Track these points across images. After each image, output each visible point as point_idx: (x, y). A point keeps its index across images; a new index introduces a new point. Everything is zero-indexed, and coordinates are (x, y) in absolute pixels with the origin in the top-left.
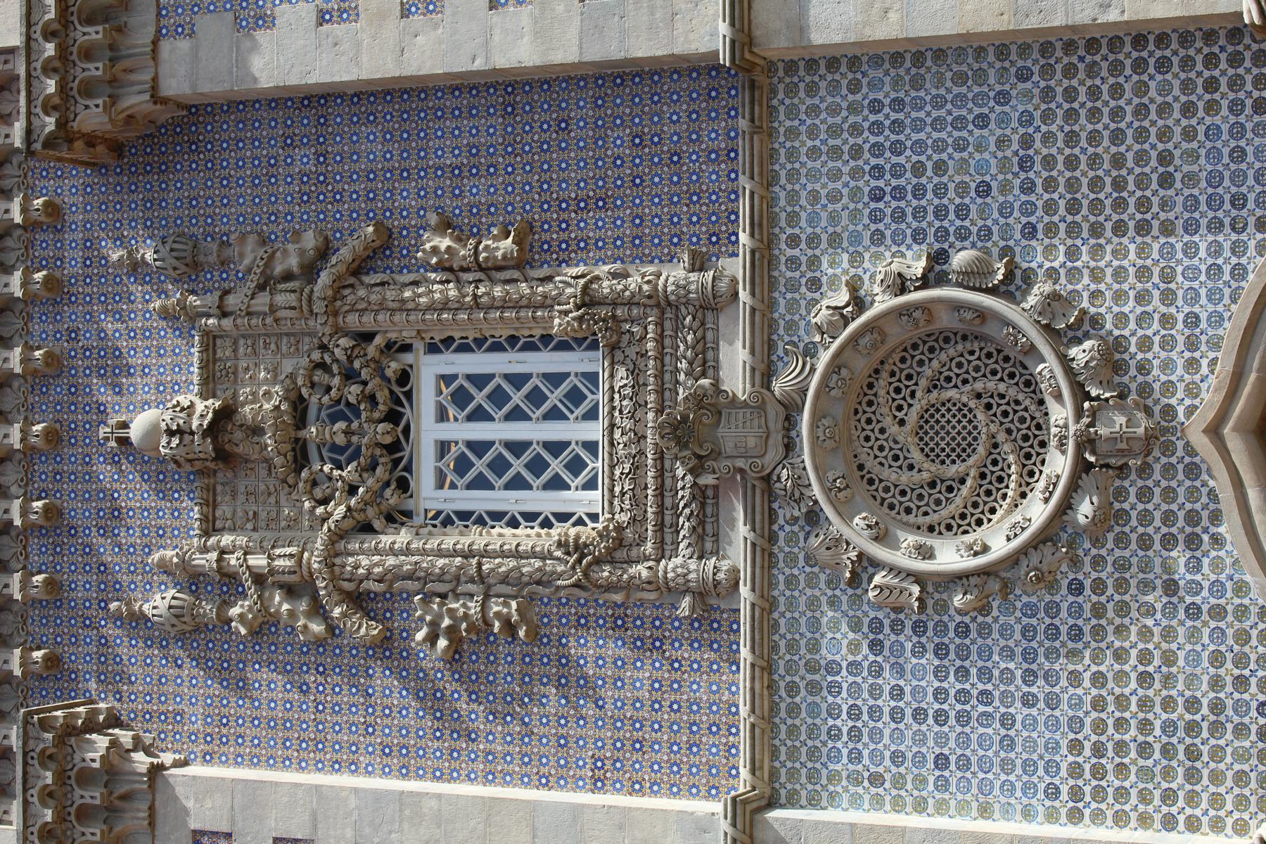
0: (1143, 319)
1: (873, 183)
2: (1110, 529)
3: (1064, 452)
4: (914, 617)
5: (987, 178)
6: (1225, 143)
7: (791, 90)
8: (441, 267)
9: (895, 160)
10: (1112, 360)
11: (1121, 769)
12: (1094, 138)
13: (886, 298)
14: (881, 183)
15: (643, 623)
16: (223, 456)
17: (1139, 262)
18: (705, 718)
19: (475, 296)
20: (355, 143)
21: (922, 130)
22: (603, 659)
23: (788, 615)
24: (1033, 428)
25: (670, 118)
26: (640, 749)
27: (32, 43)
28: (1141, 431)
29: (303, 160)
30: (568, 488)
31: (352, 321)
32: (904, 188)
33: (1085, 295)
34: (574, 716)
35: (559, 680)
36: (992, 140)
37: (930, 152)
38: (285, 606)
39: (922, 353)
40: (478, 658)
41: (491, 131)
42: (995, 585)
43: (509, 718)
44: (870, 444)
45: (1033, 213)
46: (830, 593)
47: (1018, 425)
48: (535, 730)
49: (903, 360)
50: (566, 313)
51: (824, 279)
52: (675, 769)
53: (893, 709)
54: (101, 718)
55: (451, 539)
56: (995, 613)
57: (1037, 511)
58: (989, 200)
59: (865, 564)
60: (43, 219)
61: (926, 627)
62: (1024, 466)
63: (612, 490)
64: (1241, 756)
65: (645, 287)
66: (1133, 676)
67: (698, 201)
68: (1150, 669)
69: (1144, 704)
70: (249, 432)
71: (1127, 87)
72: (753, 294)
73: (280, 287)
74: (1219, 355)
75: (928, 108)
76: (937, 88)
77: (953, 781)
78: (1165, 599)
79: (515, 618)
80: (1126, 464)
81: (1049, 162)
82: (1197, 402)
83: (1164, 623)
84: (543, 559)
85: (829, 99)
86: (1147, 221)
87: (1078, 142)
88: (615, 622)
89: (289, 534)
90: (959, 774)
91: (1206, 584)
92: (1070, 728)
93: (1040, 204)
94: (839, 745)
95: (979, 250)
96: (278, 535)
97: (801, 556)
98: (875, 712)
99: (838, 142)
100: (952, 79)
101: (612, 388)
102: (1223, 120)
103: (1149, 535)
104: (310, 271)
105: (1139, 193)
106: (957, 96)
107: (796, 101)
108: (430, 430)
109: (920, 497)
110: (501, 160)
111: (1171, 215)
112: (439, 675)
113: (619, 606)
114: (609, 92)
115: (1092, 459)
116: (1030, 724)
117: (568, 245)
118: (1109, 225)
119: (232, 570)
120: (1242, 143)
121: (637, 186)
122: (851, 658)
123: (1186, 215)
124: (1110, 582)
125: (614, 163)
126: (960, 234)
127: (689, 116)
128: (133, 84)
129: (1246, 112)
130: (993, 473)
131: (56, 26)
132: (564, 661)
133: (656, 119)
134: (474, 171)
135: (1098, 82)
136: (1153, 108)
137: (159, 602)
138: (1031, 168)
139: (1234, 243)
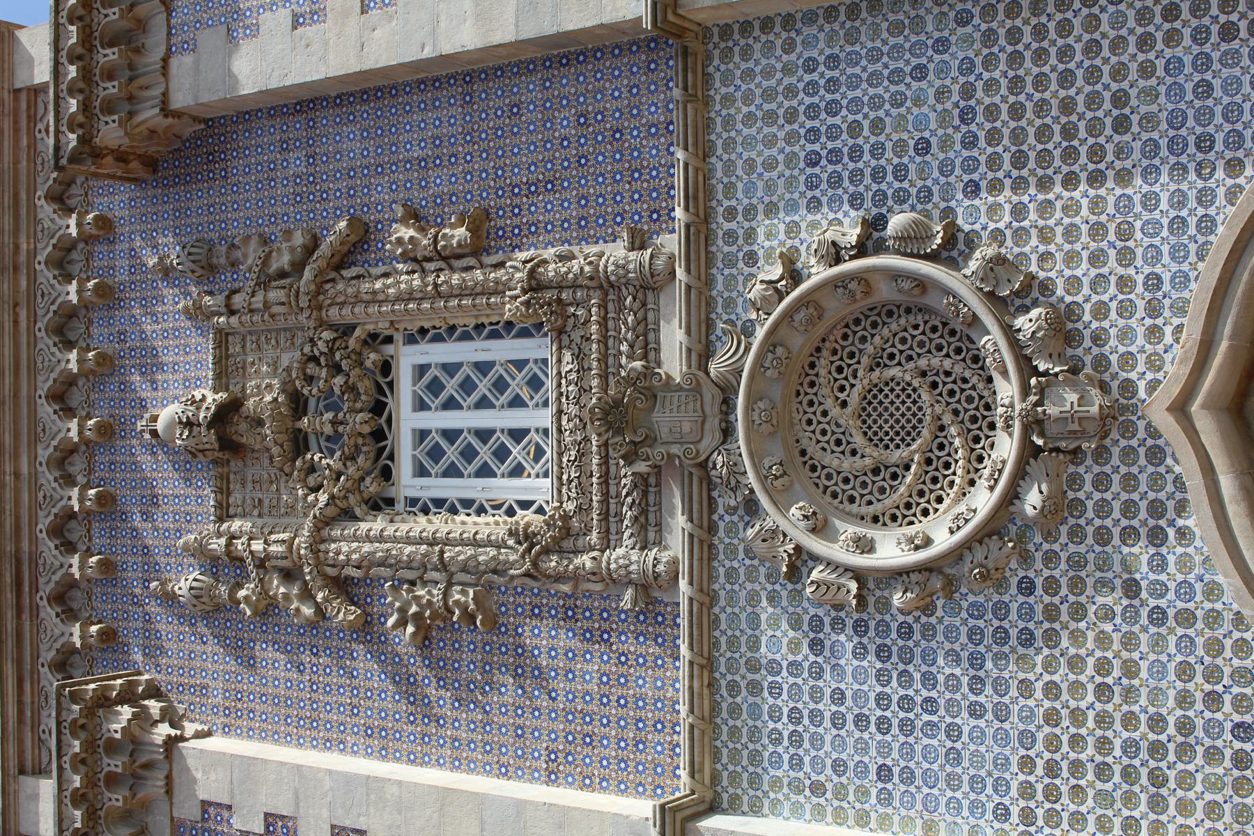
0: (1098, 283)
1: (809, 147)
2: (1064, 521)
3: (1010, 435)
4: (856, 616)
5: (927, 134)
6: (1189, 77)
7: (727, 55)
8: (405, 257)
9: (830, 121)
10: (1063, 329)
11: (1077, 791)
12: (1040, 82)
13: (821, 269)
14: (817, 147)
16: (230, 446)
18: (650, 715)
19: (436, 285)
20: (337, 142)
21: (857, 87)
22: (555, 650)
23: (729, 610)
24: (981, 409)
25: (612, 95)
26: (590, 744)
27: (61, 68)
28: (1095, 410)
29: (296, 163)
30: (495, 475)
32: (840, 150)
33: (1034, 257)
34: (530, 706)
35: (516, 670)
36: (931, 92)
37: (866, 109)
38: (282, 590)
39: (864, 329)
40: (445, 645)
41: (452, 121)
42: (937, 583)
43: (472, 706)
44: (812, 428)
45: (975, 170)
46: (769, 587)
47: (965, 405)
48: (496, 719)
49: (845, 337)
50: (516, 297)
51: (761, 253)
52: (623, 765)
53: (834, 714)
54: (140, 689)
55: (421, 525)
56: (940, 613)
57: (983, 500)
58: (928, 158)
60: (94, 232)
61: (867, 626)
62: (973, 450)
63: (560, 479)
64: (1214, 784)
65: (587, 269)
66: (1090, 687)
67: (639, 178)
68: (1109, 680)
69: (1103, 720)
70: (254, 424)
71: (1076, 22)
72: (688, 271)
73: (274, 284)
74: (1185, 321)
75: (864, 63)
76: (873, 40)
77: (897, 795)
78: (1125, 602)
80: (1080, 447)
81: (992, 112)
82: (1160, 376)
84: (499, 547)
85: (764, 62)
86: (1101, 171)
88: (566, 613)
89: (286, 520)
90: (903, 788)
91: (1172, 585)
92: (1021, 742)
93: (983, 159)
94: (780, 749)
95: (919, 213)
96: (278, 521)
97: (741, 548)
98: (815, 716)
99: (773, 106)
100: (888, 30)
101: (559, 373)
102: (1186, 50)
103: (1107, 528)
104: (298, 268)
105: (1091, 141)
106: (893, 47)
107: (731, 66)
108: (408, 420)
110: (460, 149)
112: (412, 661)
113: (569, 597)
114: (556, 72)
115: (1040, 442)
116: (978, 736)
117: (521, 230)
119: (239, 554)
120: (1208, 76)
121: (582, 166)
122: (791, 658)
124: (1064, 581)
125: (561, 144)
126: (899, 197)
127: (630, 91)
128: (148, 99)
129: (1212, 40)
130: (939, 458)
131: (80, 50)
132: (520, 650)
133: (599, 97)
134: (438, 162)
135: (1044, 19)
136: (1105, 43)
137: (184, 583)
138: (973, 120)
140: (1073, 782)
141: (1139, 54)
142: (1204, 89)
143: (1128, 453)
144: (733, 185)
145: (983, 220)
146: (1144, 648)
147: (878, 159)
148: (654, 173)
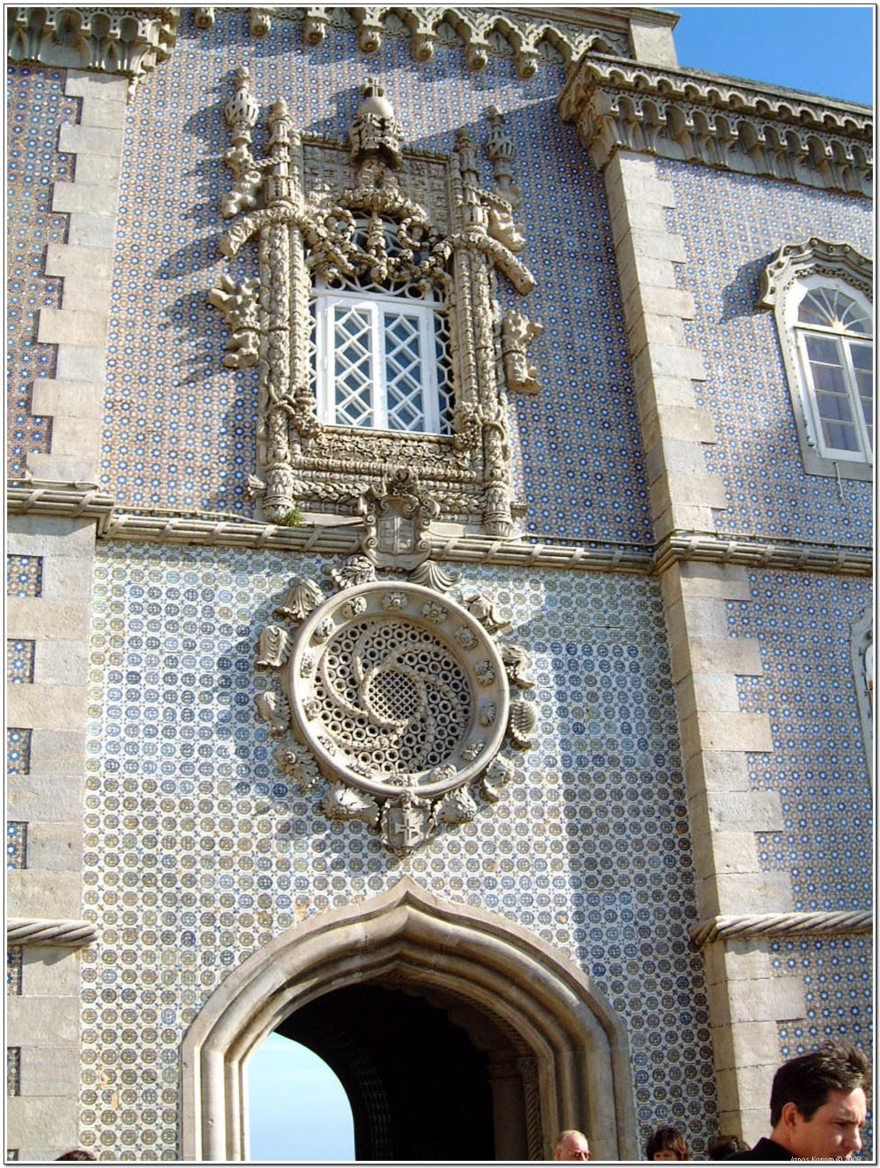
0: (490, 846)
1: (579, 647)
4: (251, 662)
5: (587, 732)
7: (641, 590)
9: (597, 664)
12: (618, 811)
16: (361, 158)
17: (532, 844)
29: (571, 243)
31: (462, 261)
49: (447, 664)
50: (476, 411)
56: (258, 726)
57: (340, 761)
58: (572, 732)
59: (295, 625)
64: (149, 918)
65: (499, 471)
68: (217, 848)
69: (188, 842)
79: (244, 350)
90: (124, 691)
91: (287, 893)
94: (145, 596)
101: (420, 441)
108: (373, 307)
115: (387, 805)
120: (619, 919)
122: (217, 609)
135: (657, 814)
136: (641, 854)
142: (611, 917)
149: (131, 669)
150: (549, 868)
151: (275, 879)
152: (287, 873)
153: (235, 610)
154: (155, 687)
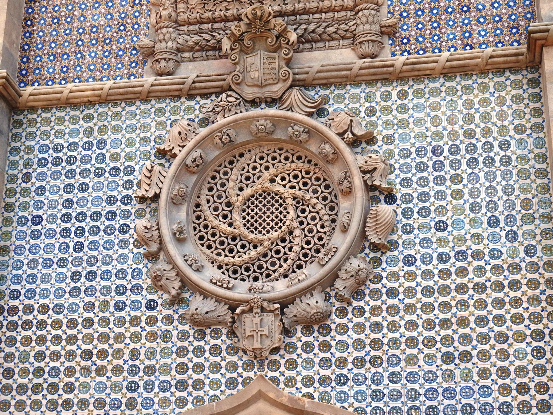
1: (446, 148)
5: (450, 229)
7: (517, 85)
9: (464, 162)
14: (446, 153)
15: (136, 17)
17: (385, 341)
18: (72, 62)
23: (138, 112)
24: (267, 272)
26: (53, 23)
36: (479, 231)
37: (470, 186)
39: (322, 192)
42: (154, 247)
44: (258, 160)
45: (423, 263)
46: (152, 138)
47: (270, 261)
49: (318, 179)
52: (40, 46)
56: (136, 250)
58: (433, 230)
61: (128, 204)
62: (241, 267)
67: (433, 27)
68: (94, 358)
69: (71, 355)
71: (521, 327)
75: (504, 183)
76: (520, 188)
82: (282, 385)
83: (126, 367)
85: (510, 112)
86: (417, 345)
87: (478, 293)
91: (152, 395)
93: (430, 267)
94: (51, 151)
97: (178, 117)
98: (71, 173)
103: (187, 354)
105: (438, 338)
107: (509, 88)
109: (219, 197)
111: (421, 363)
115: (238, 311)
118: (414, 317)
122: (108, 155)
123: (421, 374)
124: (154, 328)
126: (407, 212)
130: (236, 245)
135: (525, 305)
138: (458, 260)
139: (400, 409)
140: (34, 338)
141: (496, 369)
143: (233, 367)
144: (423, 96)
145: (389, 269)
146: (114, 379)
147: (434, 196)
148: (436, 38)
149: (35, 213)
150: (403, 364)
151: (141, 383)
152: (153, 378)
153: (123, 154)
154: (54, 226)
